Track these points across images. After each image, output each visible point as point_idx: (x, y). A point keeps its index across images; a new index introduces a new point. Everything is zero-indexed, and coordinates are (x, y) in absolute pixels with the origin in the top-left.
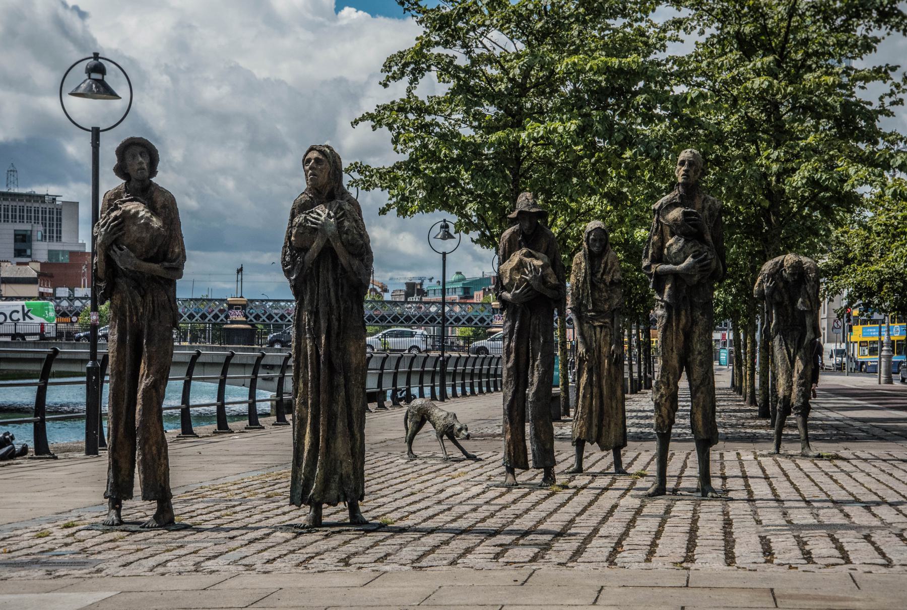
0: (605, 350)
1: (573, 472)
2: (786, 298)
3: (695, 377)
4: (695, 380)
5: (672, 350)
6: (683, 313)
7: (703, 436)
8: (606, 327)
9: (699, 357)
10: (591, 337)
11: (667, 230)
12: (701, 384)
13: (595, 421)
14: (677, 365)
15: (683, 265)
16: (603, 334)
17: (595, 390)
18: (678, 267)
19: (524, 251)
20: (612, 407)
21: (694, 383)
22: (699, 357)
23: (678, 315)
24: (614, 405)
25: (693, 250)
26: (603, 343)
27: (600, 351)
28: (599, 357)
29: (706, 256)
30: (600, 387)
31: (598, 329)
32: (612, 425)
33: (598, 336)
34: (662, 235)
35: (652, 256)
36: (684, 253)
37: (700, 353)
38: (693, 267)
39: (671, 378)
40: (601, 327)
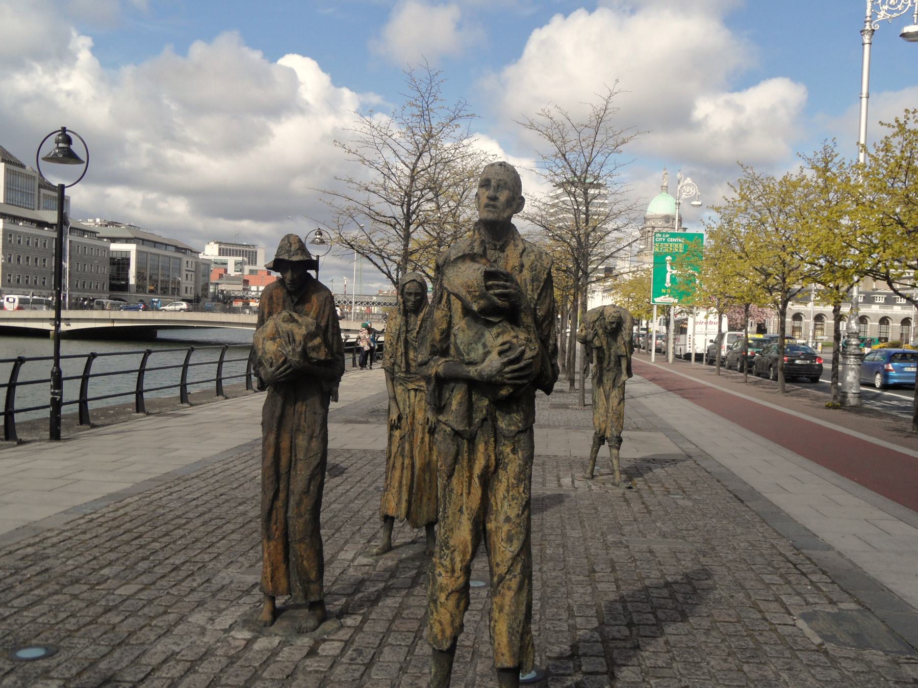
0: (420, 416)
1: (377, 554)
2: (604, 343)
3: (498, 559)
4: (498, 565)
5: (461, 511)
6: (481, 447)
7: (507, 661)
8: (421, 391)
9: (506, 527)
10: (405, 400)
11: (457, 305)
12: (509, 571)
13: (405, 497)
14: (469, 538)
15: (479, 368)
16: (418, 399)
17: (407, 461)
18: (472, 371)
19: (285, 314)
20: (425, 480)
21: (495, 569)
22: (506, 527)
23: (472, 451)
24: (427, 478)
25: (500, 340)
26: (417, 410)
27: (414, 417)
28: (412, 424)
29: (523, 352)
30: (412, 457)
31: (412, 393)
32: (425, 500)
33: (412, 401)
34: (450, 309)
35: (433, 346)
36: (484, 346)
37: (508, 519)
38: (500, 372)
39: (458, 559)
40: (416, 390)
